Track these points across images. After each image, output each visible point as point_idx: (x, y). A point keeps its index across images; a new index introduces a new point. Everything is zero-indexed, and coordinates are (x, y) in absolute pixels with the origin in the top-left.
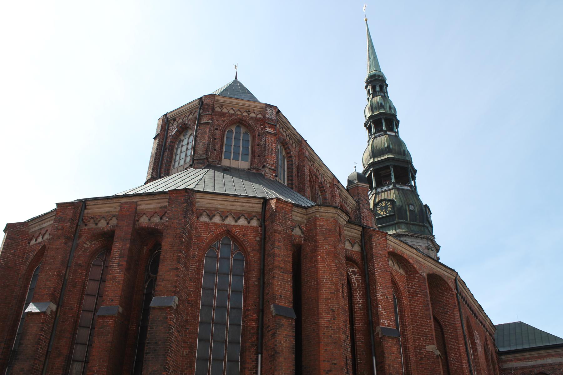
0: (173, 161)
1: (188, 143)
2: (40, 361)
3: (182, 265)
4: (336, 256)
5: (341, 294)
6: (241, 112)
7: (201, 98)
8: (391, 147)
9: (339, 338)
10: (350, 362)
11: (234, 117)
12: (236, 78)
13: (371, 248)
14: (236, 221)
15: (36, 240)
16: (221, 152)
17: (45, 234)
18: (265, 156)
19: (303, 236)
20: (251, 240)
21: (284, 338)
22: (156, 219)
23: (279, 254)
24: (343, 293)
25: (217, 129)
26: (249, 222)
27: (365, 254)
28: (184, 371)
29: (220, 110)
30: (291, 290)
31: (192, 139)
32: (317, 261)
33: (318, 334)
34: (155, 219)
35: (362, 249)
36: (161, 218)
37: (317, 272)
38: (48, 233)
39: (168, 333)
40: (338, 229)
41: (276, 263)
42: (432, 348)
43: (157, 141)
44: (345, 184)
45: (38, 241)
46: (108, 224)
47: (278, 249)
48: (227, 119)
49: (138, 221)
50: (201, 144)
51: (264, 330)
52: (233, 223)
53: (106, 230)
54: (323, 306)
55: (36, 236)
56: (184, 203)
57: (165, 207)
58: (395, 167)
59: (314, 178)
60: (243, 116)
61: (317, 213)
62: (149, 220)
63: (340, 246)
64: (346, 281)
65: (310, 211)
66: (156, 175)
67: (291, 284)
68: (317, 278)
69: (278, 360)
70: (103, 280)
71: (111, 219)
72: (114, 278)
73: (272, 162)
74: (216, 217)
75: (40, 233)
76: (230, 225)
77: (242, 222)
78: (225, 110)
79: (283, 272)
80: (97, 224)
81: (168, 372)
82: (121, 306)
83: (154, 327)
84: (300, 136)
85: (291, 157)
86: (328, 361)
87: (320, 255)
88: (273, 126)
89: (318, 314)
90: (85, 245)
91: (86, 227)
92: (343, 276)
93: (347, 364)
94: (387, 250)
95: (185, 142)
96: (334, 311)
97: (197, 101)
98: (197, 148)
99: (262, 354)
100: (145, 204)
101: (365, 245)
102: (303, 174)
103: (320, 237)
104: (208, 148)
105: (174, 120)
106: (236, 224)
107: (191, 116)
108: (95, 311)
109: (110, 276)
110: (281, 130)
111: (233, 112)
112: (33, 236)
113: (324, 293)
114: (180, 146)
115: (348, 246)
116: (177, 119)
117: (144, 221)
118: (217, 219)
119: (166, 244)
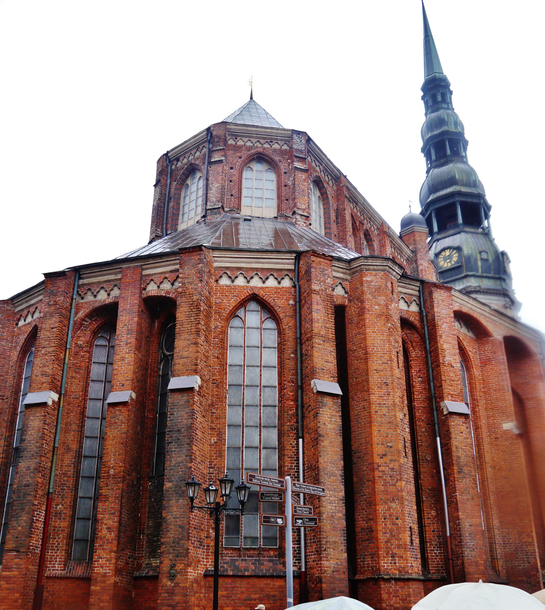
0: (181, 213)
1: (198, 189)
2: (47, 458)
3: (203, 338)
4: (388, 318)
5: (395, 364)
6: (261, 143)
7: (208, 129)
8: (457, 177)
9: (395, 415)
10: (408, 444)
11: (253, 151)
12: (251, 98)
13: (433, 307)
14: (264, 282)
15: (25, 320)
16: (240, 198)
17: (34, 312)
18: (294, 199)
19: (346, 296)
20: (283, 305)
21: (329, 419)
22: (166, 286)
23: (318, 320)
24: (398, 363)
25: (232, 168)
26: (279, 283)
27: (424, 314)
28: (213, 462)
29: (234, 143)
30: (335, 362)
31: (201, 183)
32: (364, 326)
33: (370, 412)
34: (165, 285)
35: (420, 309)
36: (173, 284)
37: (365, 339)
38: (37, 311)
39: (192, 419)
40: (389, 284)
41: (316, 331)
42: (509, 426)
43: (158, 189)
44: (396, 228)
45: (27, 322)
46: (109, 295)
47: (317, 313)
48: (245, 154)
49: (145, 289)
50: (214, 189)
51: (304, 410)
52: (260, 284)
53: (107, 302)
54: (374, 379)
55: (24, 315)
56: (199, 264)
57: (177, 270)
58: (463, 204)
59: (358, 224)
60: (264, 148)
61: (363, 267)
62: (159, 287)
63: (393, 305)
64: (401, 349)
65: (355, 265)
66: (162, 232)
67: (334, 354)
68: (366, 346)
69: (322, 444)
70: (109, 363)
71: (112, 290)
72: (123, 359)
73: (303, 207)
74: (238, 278)
75: (29, 312)
76: (256, 287)
77: (271, 283)
78: (240, 143)
79: (324, 341)
80: (95, 296)
81: (195, 463)
82: (134, 391)
83: (175, 413)
84: (338, 170)
85: (327, 198)
86: (382, 444)
87: (369, 318)
88: (302, 160)
89: (369, 389)
90: (84, 322)
91: (82, 301)
92: (398, 342)
93: (405, 447)
94: (451, 309)
95: (193, 188)
96: (387, 385)
97: (205, 133)
98: (209, 195)
99: (303, 438)
100: (151, 268)
101: (424, 304)
102: (344, 220)
103: (368, 296)
104: (222, 194)
105: (178, 160)
106: (264, 286)
107: (198, 153)
108: (104, 399)
109: (118, 357)
110: (313, 164)
111: (251, 144)
112: (21, 315)
113: (375, 364)
114: (188, 193)
115: (403, 305)
116: (181, 159)
117: (152, 289)
118: (240, 281)
119: (182, 314)
